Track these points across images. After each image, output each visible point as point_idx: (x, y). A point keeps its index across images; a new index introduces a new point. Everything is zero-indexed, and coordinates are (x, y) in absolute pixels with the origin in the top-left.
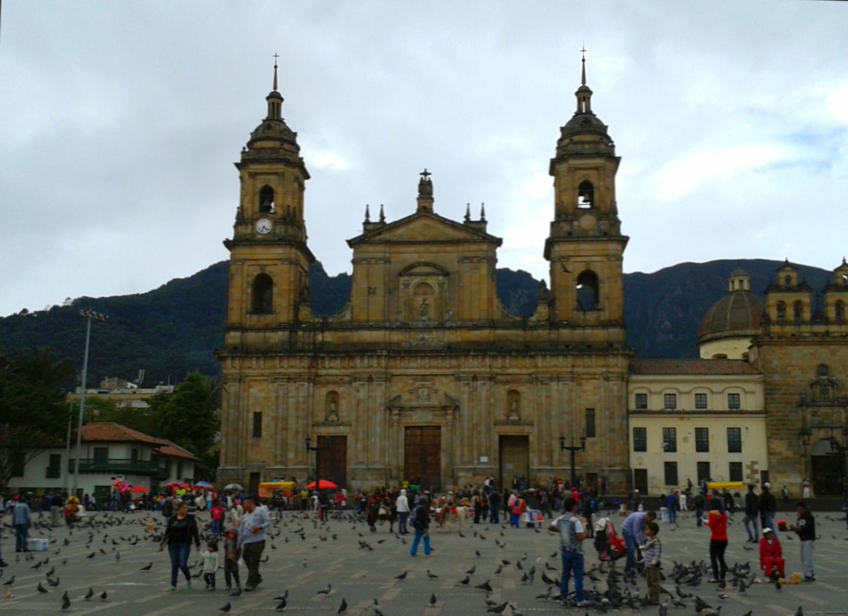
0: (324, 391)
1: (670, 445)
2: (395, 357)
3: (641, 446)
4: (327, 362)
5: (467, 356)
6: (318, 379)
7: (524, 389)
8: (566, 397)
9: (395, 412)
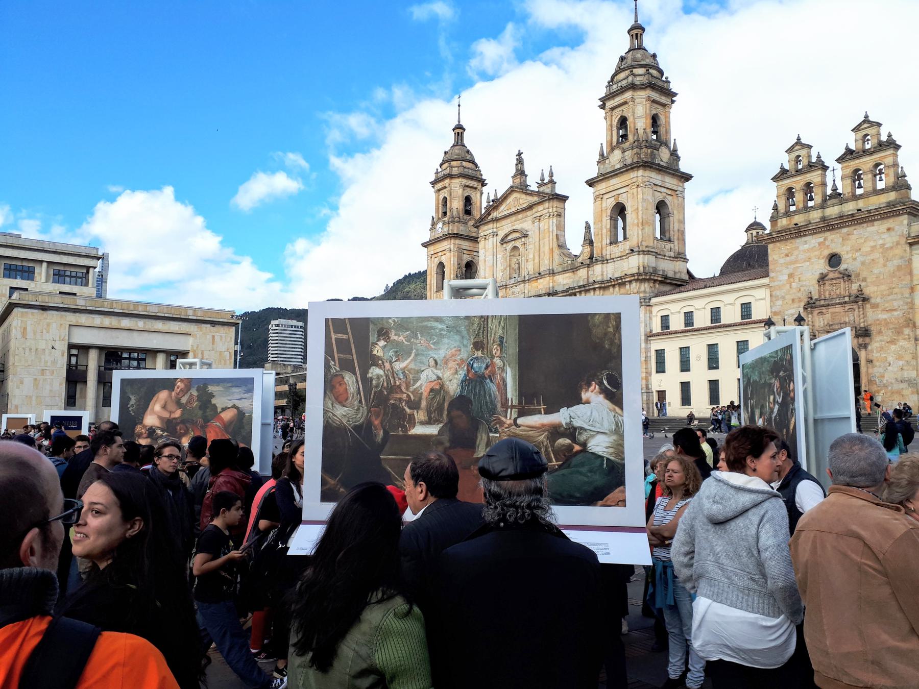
1: (685, 366)
3: (661, 368)
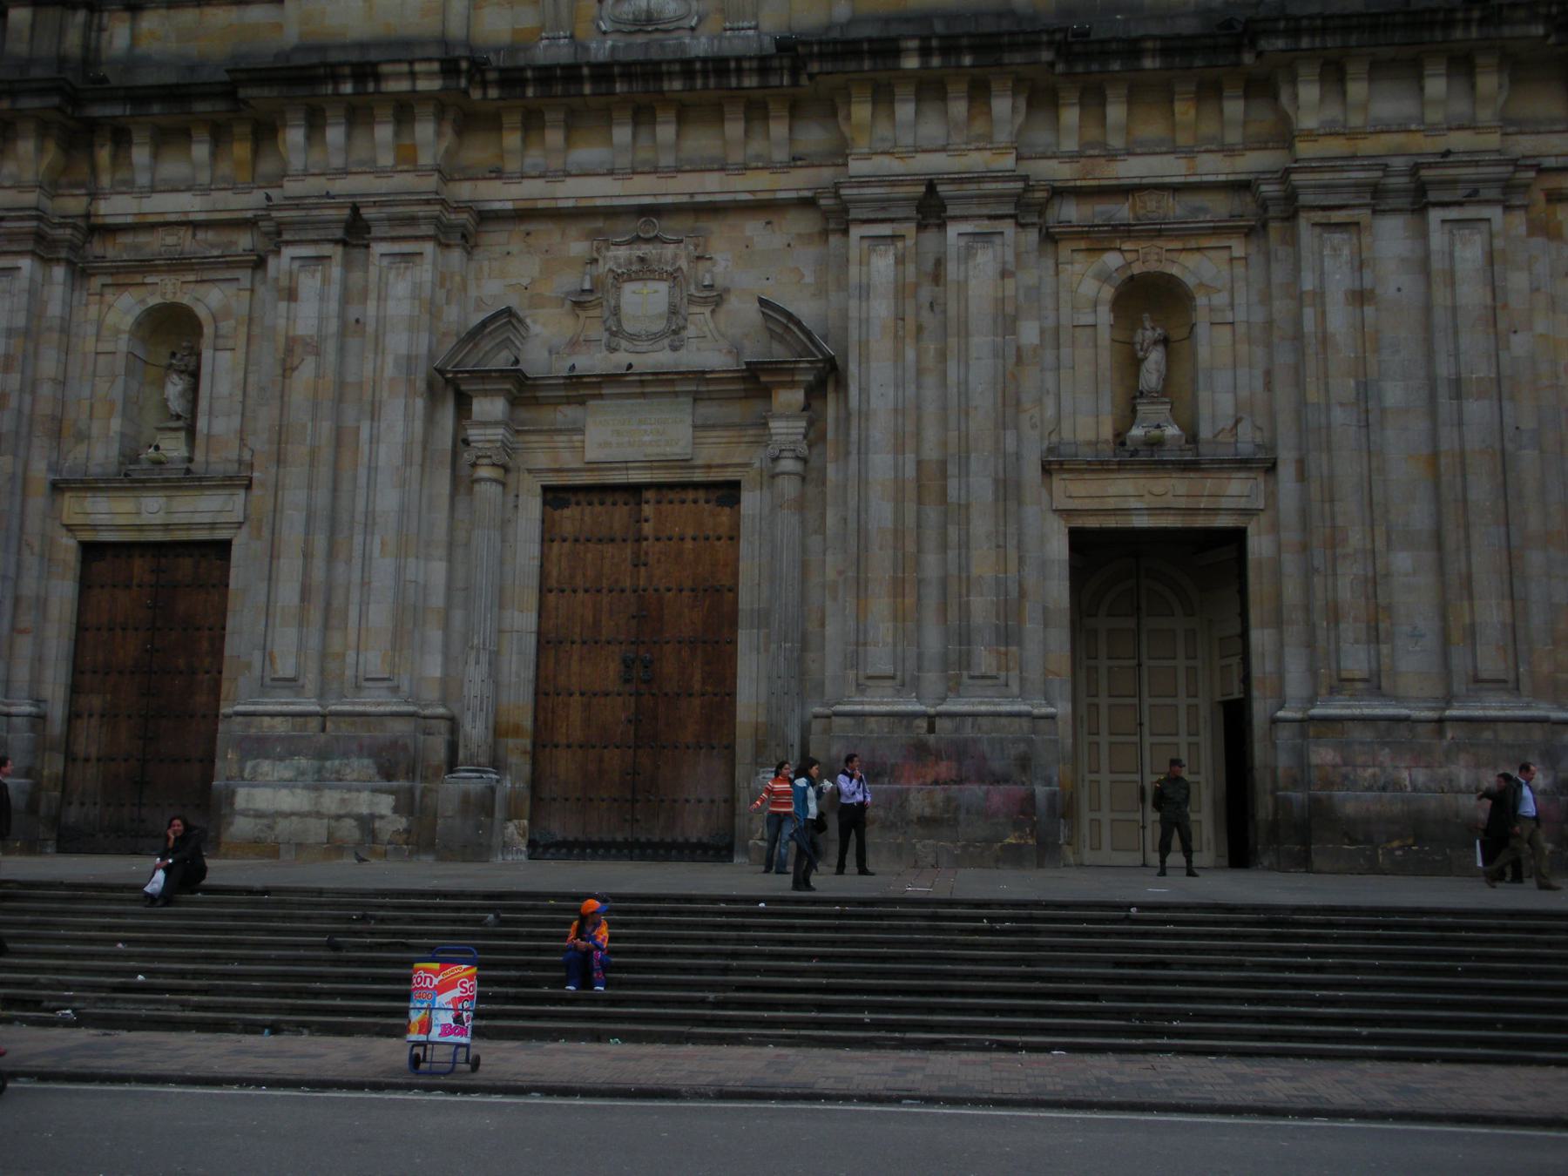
0: (125, 308)
2: (491, 122)
4: (140, 154)
5: (883, 96)
6: (97, 247)
7: (1198, 268)
8: (1472, 294)
9: (490, 407)
